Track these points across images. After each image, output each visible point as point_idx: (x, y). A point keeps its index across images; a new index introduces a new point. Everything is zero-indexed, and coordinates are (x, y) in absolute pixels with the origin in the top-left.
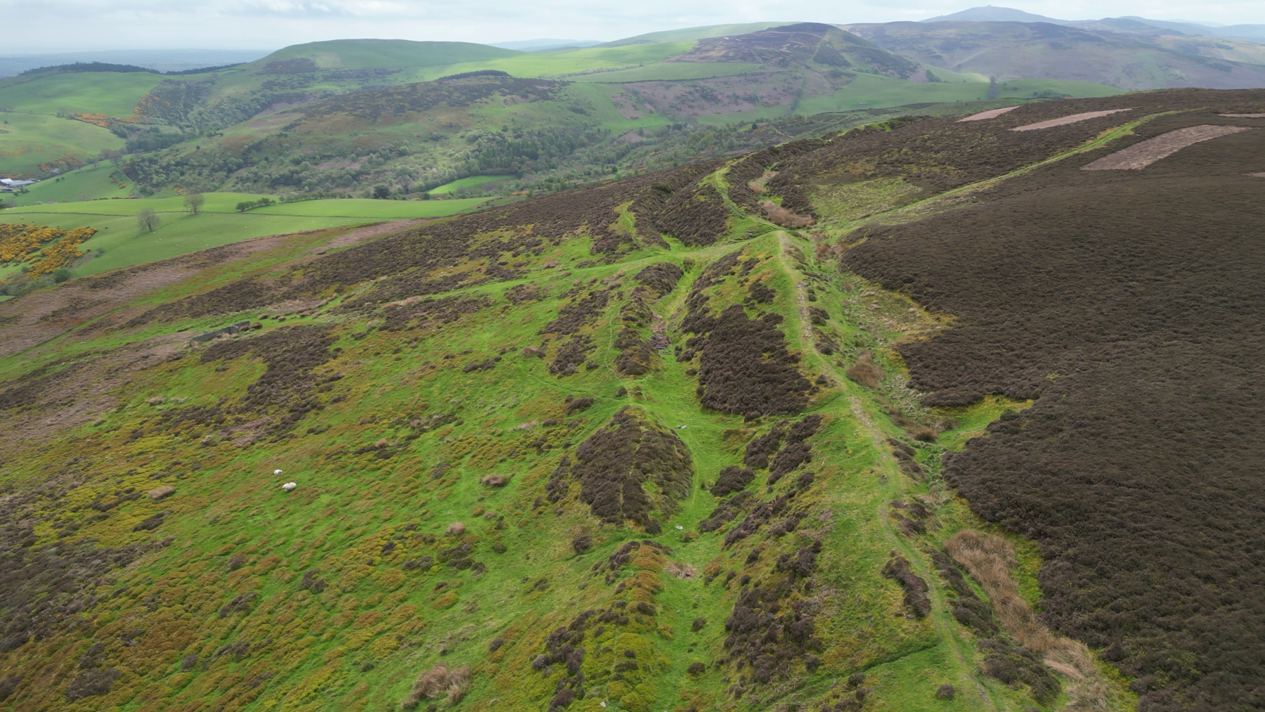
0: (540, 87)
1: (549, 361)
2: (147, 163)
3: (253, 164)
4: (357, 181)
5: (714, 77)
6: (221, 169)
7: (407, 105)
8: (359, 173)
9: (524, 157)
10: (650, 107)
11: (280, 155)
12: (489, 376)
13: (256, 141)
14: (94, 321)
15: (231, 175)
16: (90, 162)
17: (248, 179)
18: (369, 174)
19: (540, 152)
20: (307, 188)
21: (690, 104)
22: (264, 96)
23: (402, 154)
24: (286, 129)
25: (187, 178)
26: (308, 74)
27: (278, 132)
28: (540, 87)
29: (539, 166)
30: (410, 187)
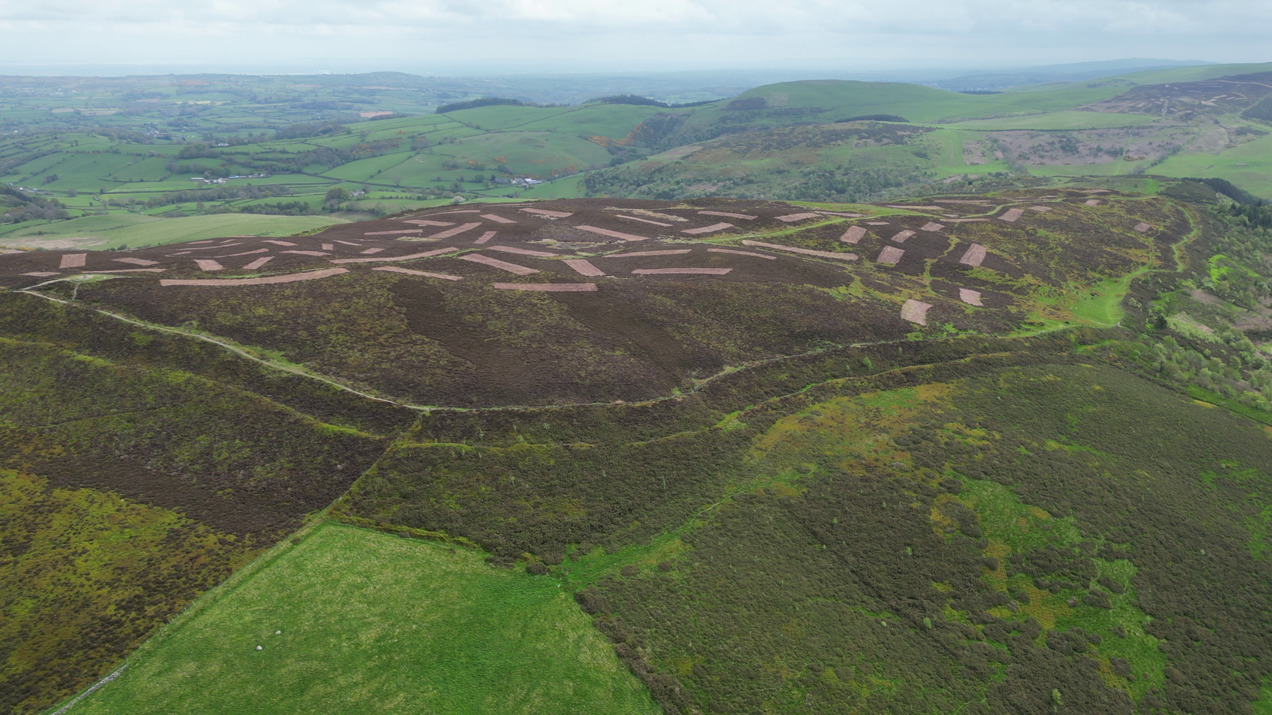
0: (899, 133)
3: (653, 182)
5: (1093, 129)
7: (775, 144)
9: (833, 191)
10: (999, 154)
13: (660, 166)
16: (581, 171)
21: (1042, 153)
22: (717, 128)
23: (750, 182)
24: (684, 158)
25: (614, 189)
26: (756, 111)
27: (675, 161)
28: (899, 133)
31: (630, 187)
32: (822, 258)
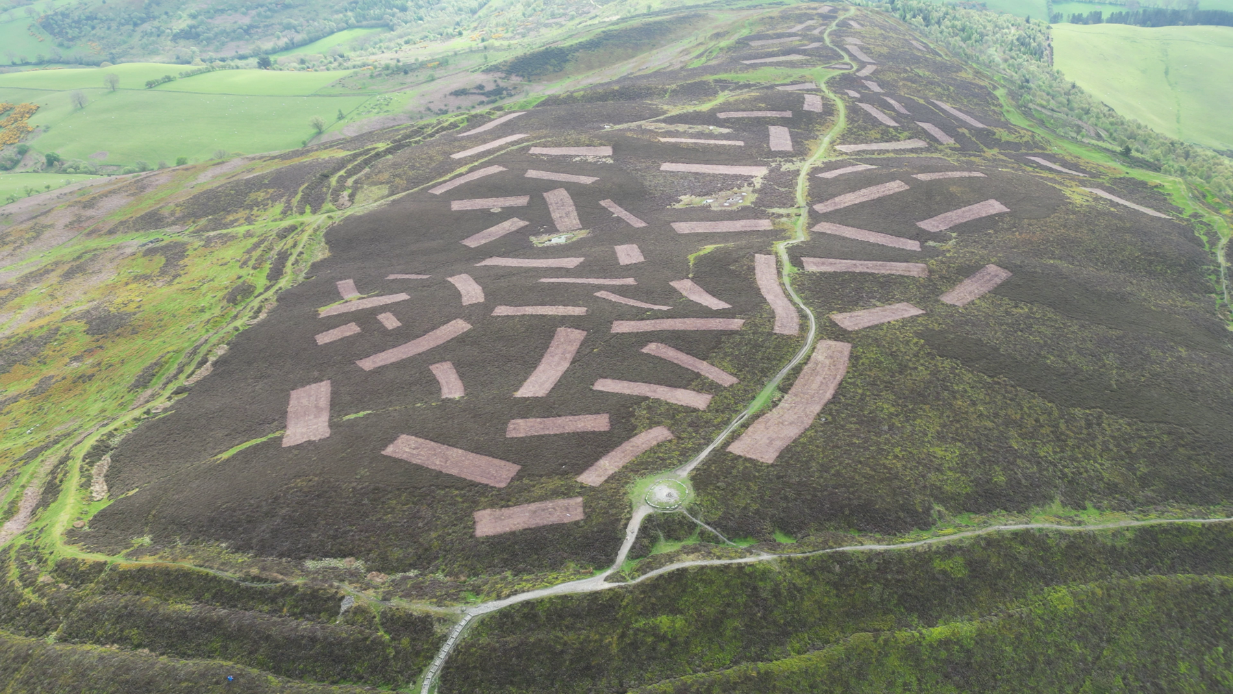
1: (240, 264)
2: (60, 17)
3: (154, 18)
4: (249, 34)
6: (127, 23)
8: (250, 27)
9: (395, 10)
11: (178, 8)
12: (225, 267)
14: (91, 228)
15: (137, 29)
17: (151, 34)
18: (258, 27)
19: (410, 4)
20: (205, 42)
25: (97, 31)
29: (409, 18)
30: (295, 40)
31: (124, 28)
32: (895, 151)
